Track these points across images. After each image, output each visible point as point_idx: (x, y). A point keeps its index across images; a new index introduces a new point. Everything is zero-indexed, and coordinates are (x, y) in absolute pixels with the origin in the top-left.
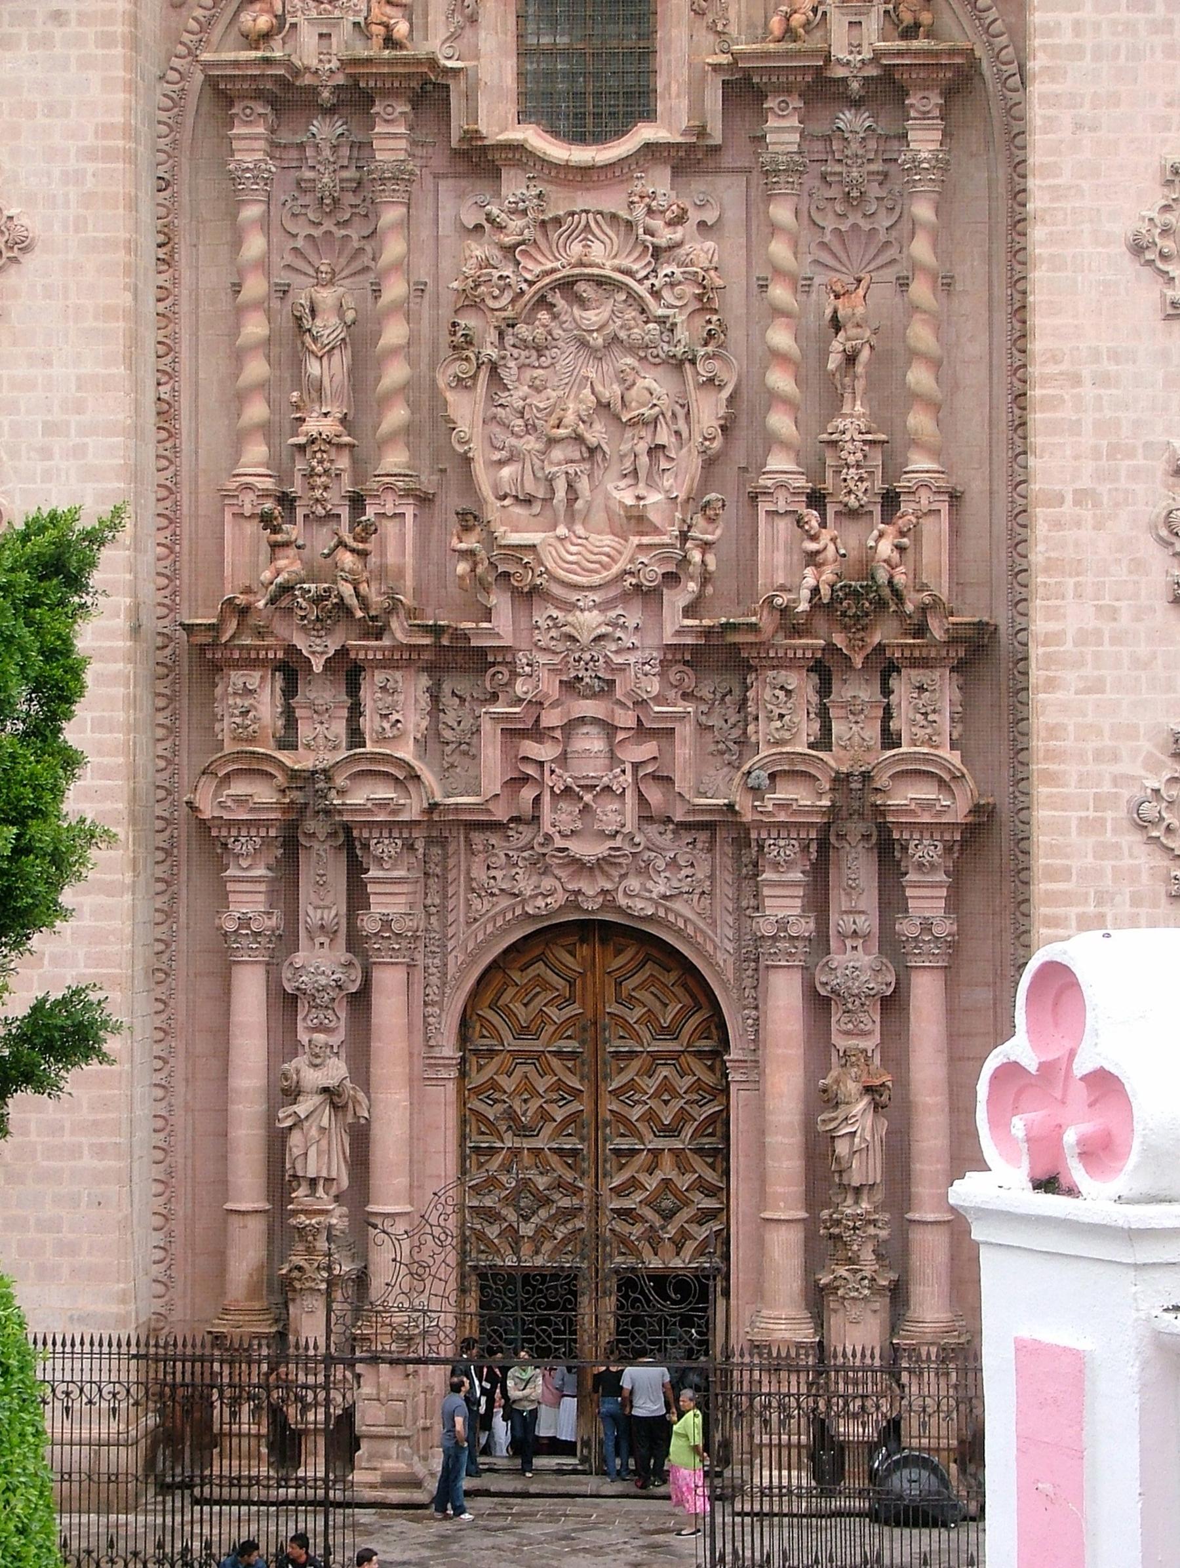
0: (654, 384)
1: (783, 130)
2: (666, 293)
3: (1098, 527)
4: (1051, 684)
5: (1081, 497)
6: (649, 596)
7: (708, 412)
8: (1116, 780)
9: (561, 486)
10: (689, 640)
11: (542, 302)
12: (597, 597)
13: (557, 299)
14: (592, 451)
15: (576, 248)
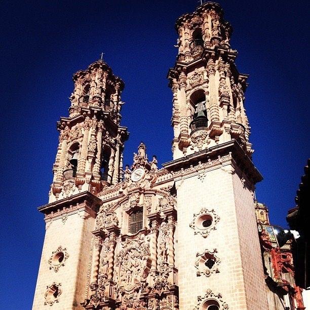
0: (139, 260)
1: (154, 225)
2: (141, 249)
3: (187, 266)
4: (182, 292)
5: (185, 262)
6: (137, 291)
7: (145, 262)
8: (191, 306)
9: (128, 277)
10: (142, 297)
11: (127, 253)
12: (131, 292)
13: (128, 252)
14: (132, 272)
15: (131, 246)
